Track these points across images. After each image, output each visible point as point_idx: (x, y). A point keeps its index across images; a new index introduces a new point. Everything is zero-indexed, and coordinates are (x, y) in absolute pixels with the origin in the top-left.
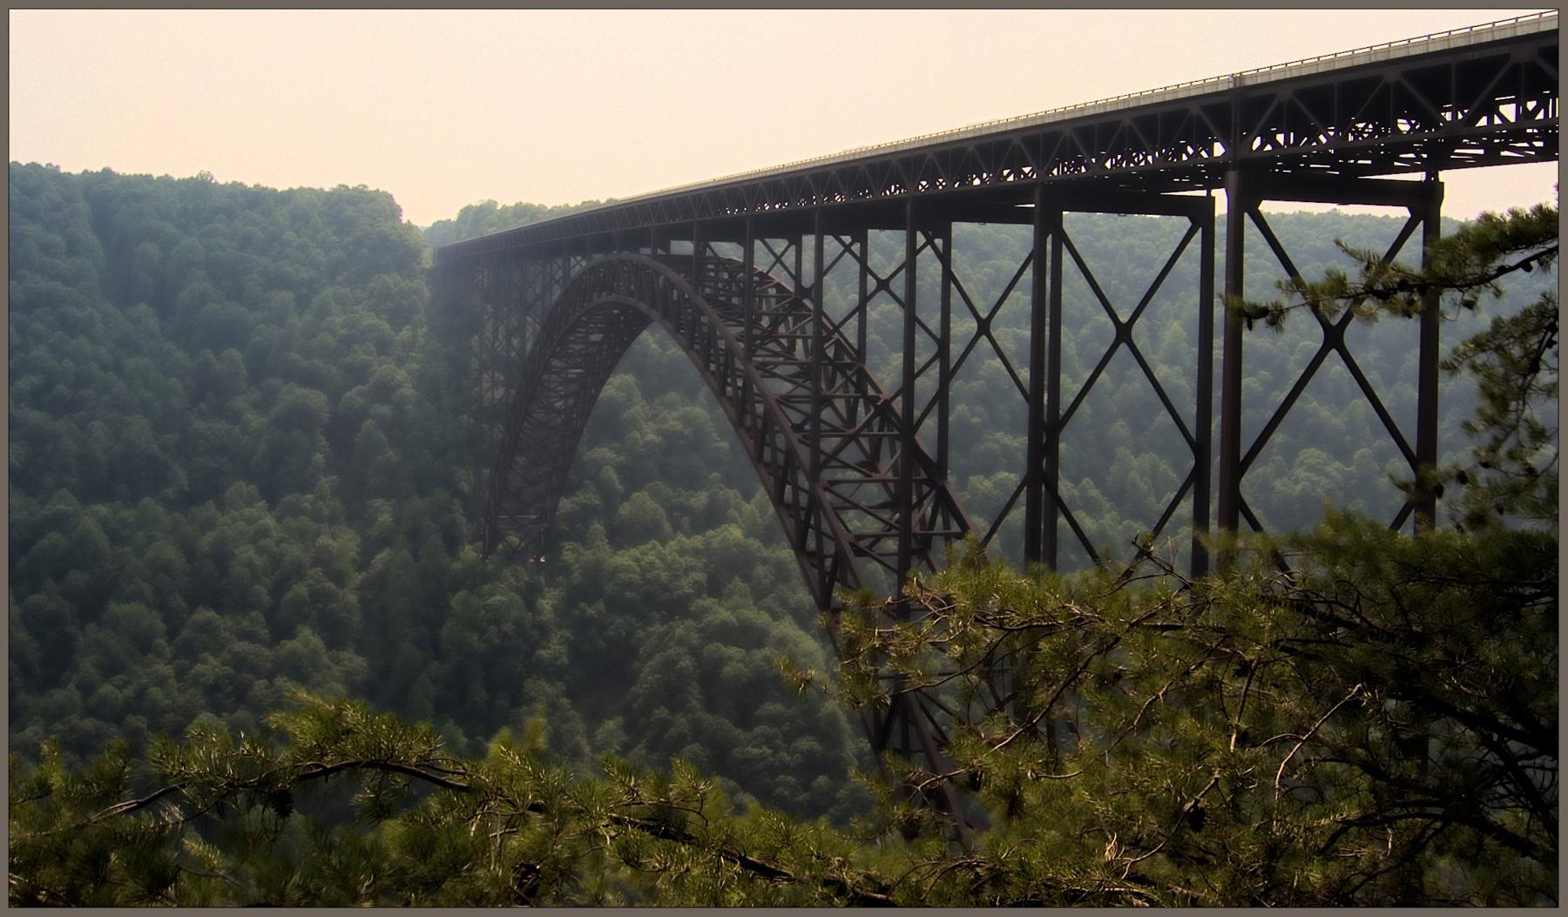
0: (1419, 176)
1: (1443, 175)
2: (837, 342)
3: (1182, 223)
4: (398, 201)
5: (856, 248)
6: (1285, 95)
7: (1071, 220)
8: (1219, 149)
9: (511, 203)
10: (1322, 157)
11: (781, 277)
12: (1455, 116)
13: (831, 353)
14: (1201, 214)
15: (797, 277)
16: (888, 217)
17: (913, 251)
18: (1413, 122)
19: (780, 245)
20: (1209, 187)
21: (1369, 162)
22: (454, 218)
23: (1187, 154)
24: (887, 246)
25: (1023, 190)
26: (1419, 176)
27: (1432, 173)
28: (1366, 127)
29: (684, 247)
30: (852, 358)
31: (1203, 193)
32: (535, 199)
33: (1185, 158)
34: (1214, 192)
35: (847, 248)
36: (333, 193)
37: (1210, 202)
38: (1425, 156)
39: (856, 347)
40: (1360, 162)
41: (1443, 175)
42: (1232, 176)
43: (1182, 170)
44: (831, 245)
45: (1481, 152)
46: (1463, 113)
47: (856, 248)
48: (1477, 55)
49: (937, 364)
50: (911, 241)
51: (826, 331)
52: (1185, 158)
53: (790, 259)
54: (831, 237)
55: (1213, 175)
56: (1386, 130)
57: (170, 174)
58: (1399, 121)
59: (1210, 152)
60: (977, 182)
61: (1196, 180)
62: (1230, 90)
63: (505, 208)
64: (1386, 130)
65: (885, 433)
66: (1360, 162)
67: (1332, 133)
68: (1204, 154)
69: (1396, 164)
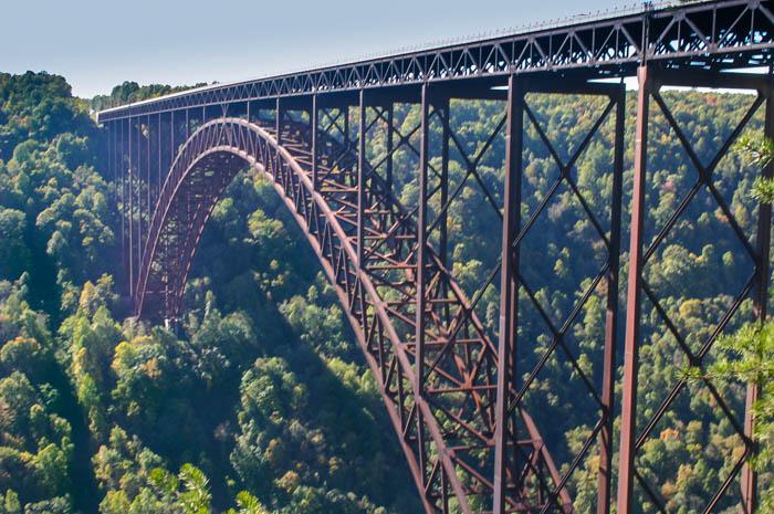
2: (373, 178)
3: (606, 100)
5: (385, 114)
6: (680, 17)
7: (529, 98)
10: (702, 58)
11: (334, 131)
13: (369, 182)
14: (617, 94)
15: (346, 134)
16: (409, 94)
17: (427, 117)
19: (335, 112)
20: (622, 76)
24: (412, 117)
25: (503, 80)
29: (274, 113)
31: (617, 80)
33: (607, 58)
34: (627, 80)
35: (380, 115)
37: (622, 85)
39: (385, 178)
42: (642, 70)
43: (604, 67)
44: (371, 113)
47: (385, 114)
51: (369, 172)
52: (607, 58)
53: (341, 121)
54: (370, 108)
55: (630, 69)
61: (613, 70)
65: (405, 236)
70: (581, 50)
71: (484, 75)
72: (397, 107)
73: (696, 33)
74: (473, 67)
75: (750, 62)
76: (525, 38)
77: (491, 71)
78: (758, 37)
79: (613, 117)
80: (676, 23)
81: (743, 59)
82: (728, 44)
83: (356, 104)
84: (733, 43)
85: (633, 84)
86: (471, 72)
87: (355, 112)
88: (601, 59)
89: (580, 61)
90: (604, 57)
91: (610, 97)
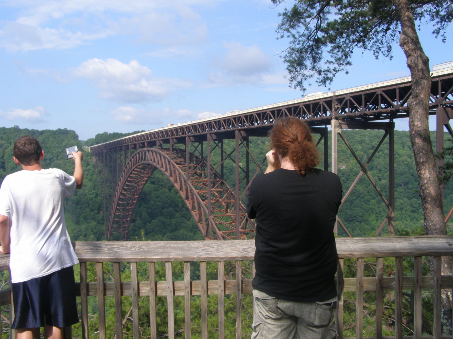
0: (387, 121)
1: (395, 120)
4: (77, 133)
5: (220, 145)
6: (347, 98)
8: (328, 113)
9: (112, 132)
11: (197, 154)
12: (397, 103)
15: (202, 153)
16: (231, 135)
18: (386, 105)
19: (197, 144)
21: (373, 117)
22: (94, 138)
23: (319, 115)
26: (387, 121)
27: (391, 120)
28: (372, 106)
30: (219, 178)
31: (324, 126)
32: (119, 131)
33: (318, 116)
34: (328, 126)
35: (217, 145)
36: (63, 130)
37: (326, 129)
38: (389, 115)
39: (220, 174)
40: (370, 117)
41: (395, 120)
45: (405, 113)
46: (400, 102)
48: (403, 86)
49: (246, 179)
50: (237, 142)
55: (328, 122)
56: (378, 107)
57: (5, 127)
58: (382, 104)
59: (326, 115)
60: (256, 124)
62: (332, 96)
63: (110, 134)
64: (378, 107)
66: (370, 117)
67: (361, 109)
68: (324, 115)
69: (381, 117)
70: (306, 113)
71: (264, 125)
72: (226, 141)
73: (356, 105)
74: (258, 122)
75: (381, 117)
76: (280, 108)
77: (266, 123)
78: (383, 106)
79: (323, 141)
80: (347, 101)
81: (377, 116)
82: (370, 110)
83: (206, 139)
84: (373, 109)
85: (329, 127)
86: (258, 124)
87: (205, 143)
88: (316, 117)
89: (306, 118)
90: (317, 117)
91: (321, 134)
